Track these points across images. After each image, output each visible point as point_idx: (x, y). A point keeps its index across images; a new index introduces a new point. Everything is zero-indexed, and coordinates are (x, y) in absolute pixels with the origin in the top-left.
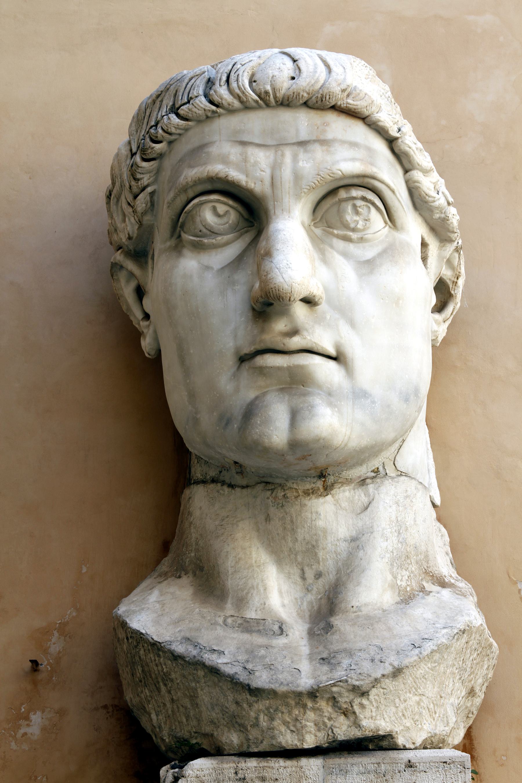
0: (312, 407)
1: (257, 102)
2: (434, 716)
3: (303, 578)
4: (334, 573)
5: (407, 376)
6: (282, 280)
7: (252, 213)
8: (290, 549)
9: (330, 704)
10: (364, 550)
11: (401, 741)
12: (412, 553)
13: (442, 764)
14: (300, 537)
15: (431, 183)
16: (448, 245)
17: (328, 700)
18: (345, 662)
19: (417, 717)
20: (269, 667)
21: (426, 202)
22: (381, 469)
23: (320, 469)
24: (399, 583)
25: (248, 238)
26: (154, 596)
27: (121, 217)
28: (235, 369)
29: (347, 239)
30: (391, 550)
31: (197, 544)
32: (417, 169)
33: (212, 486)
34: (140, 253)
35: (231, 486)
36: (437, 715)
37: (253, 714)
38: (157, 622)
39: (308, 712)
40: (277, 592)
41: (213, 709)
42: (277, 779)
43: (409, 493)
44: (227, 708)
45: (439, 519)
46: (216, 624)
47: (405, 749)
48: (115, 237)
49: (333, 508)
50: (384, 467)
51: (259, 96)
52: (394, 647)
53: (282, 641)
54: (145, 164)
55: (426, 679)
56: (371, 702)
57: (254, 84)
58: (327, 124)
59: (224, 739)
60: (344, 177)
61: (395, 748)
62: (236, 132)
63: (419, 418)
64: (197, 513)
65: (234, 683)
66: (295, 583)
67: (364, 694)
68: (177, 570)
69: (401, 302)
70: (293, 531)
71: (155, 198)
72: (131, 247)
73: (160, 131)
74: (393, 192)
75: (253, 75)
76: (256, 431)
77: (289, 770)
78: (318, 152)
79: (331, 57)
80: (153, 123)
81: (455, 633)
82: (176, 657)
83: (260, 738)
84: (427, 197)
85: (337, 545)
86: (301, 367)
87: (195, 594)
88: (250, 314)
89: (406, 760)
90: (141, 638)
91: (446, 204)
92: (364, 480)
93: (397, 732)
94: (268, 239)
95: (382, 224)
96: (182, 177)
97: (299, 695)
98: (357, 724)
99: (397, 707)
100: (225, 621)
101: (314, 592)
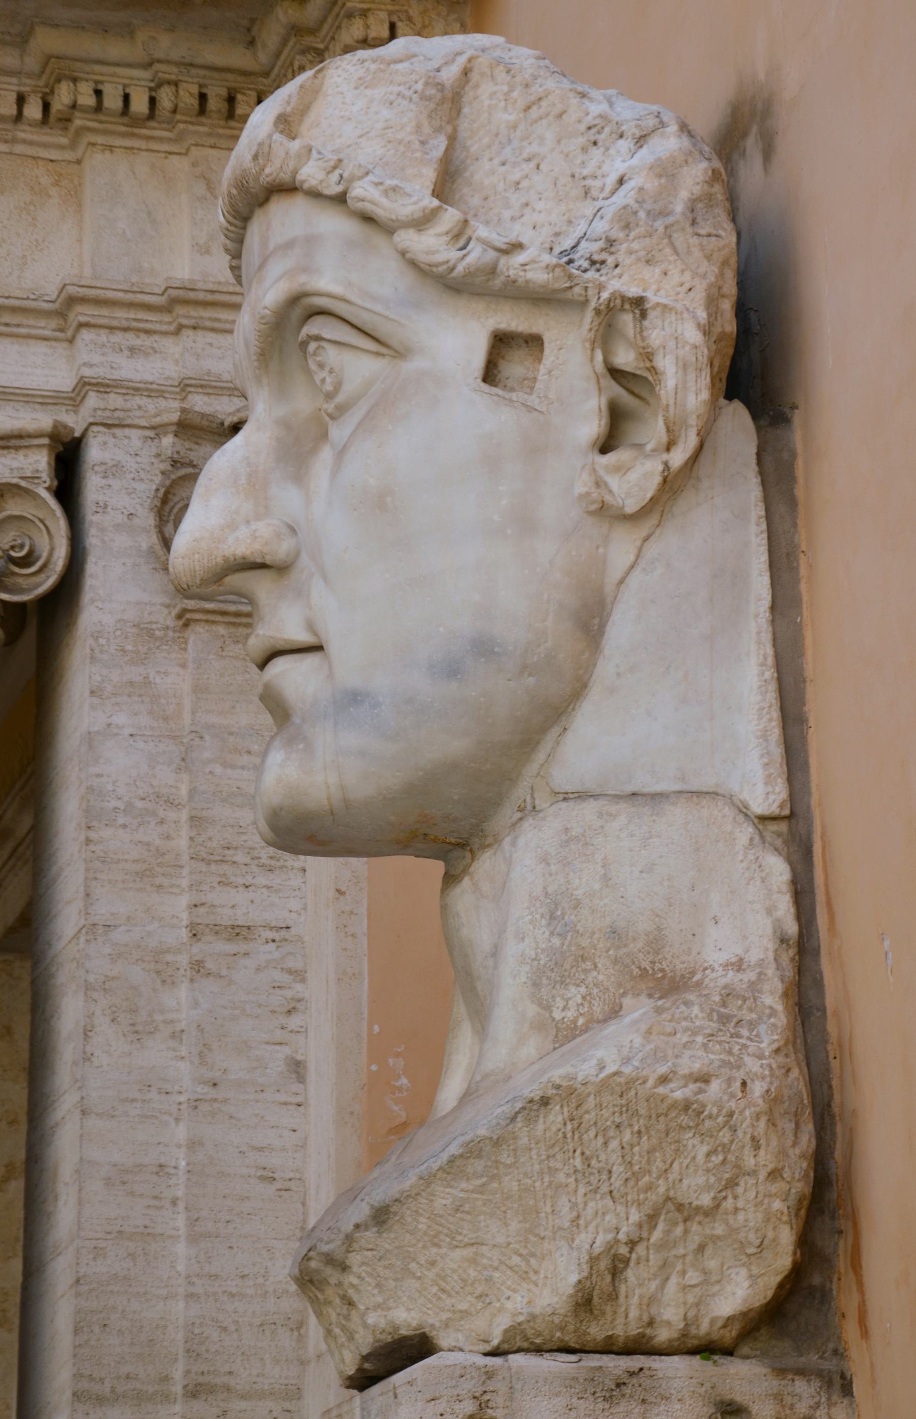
2: (534, 1278)
5: (441, 629)
12: (601, 945)
19: (479, 1289)
24: (557, 1015)
30: (533, 956)
32: (399, 228)
36: (542, 1276)
55: (467, 1213)
69: (389, 499)
81: (517, 1109)
84: (434, 269)
91: (491, 254)
93: (432, 1325)
99: (419, 1278)
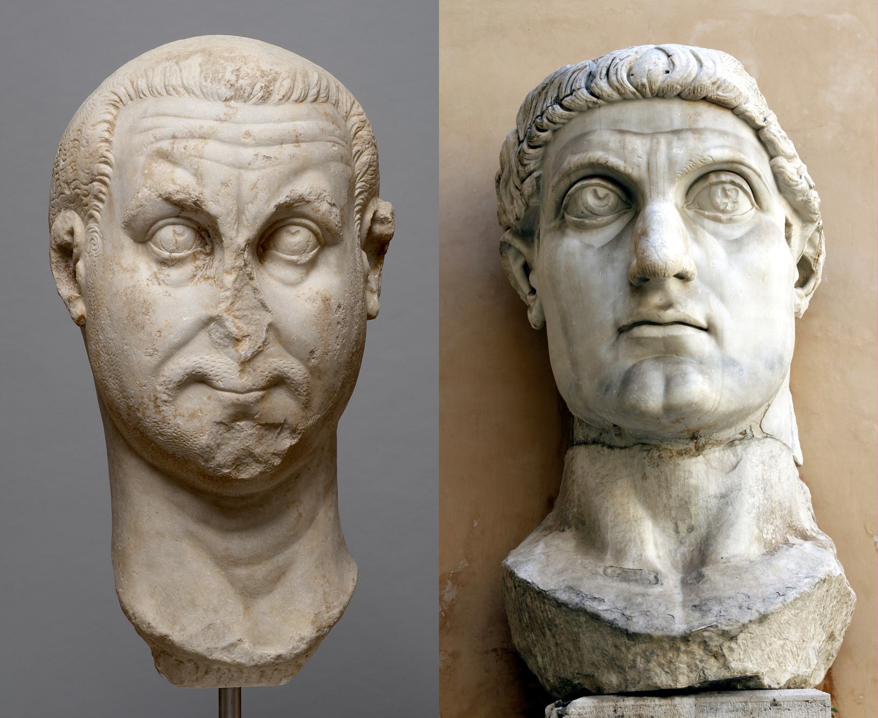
0: (685, 374)
1: (634, 94)
3: (677, 531)
4: (705, 527)
6: (657, 258)
7: (630, 196)
11: (766, 681)
14: (674, 494)
15: (795, 169)
16: (810, 225)
17: (700, 644)
18: (716, 609)
19: (781, 660)
20: (646, 613)
21: (790, 186)
22: (748, 431)
23: (691, 432)
25: (626, 219)
26: (540, 548)
27: (509, 200)
28: (614, 339)
29: (717, 220)
31: (579, 500)
33: (593, 447)
34: (527, 233)
35: (611, 447)
37: (630, 657)
38: (542, 572)
39: (681, 655)
40: (653, 545)
41: (594, 651)
43: (774, 453)
45: (802, 477)
46: (596, 573)
47: (770, 688)
48: (504, 218)
49: (704, 466)
51: (636, 89)
52: (760, 595)
53: (657, 589)
54: (531, 151)
56: (739, 646)
57: (632, 77)
58: (698, 114)
59: (604, 680)
60: (715, 163)
61: (761, 688)
62: (616, 122)
63: (784, 384)
64: (579, 472)
66: (670, 536)
67: (733, 638)
68: (560, 524)
70: (668, 488)
71: (541, 182)
72: (519, 228)
73: (545, 120)
74: (760, 176)
75: (630, 69)
76: (633, 397)
77: (664, 708)
78: (691, 140)
79: (702, 52)
80: (539, 113)
82: (560, 605)
83: (638, 679)
86: (675, 338)
87: (577, 546)
88: (628, 289)
89: (771, 699)
92: (733, 442)
94: (644, 220)
95: (750, 206)
96: (566, 163)
97: (673, 639)
100: (605, 571)
101: (687, 545)
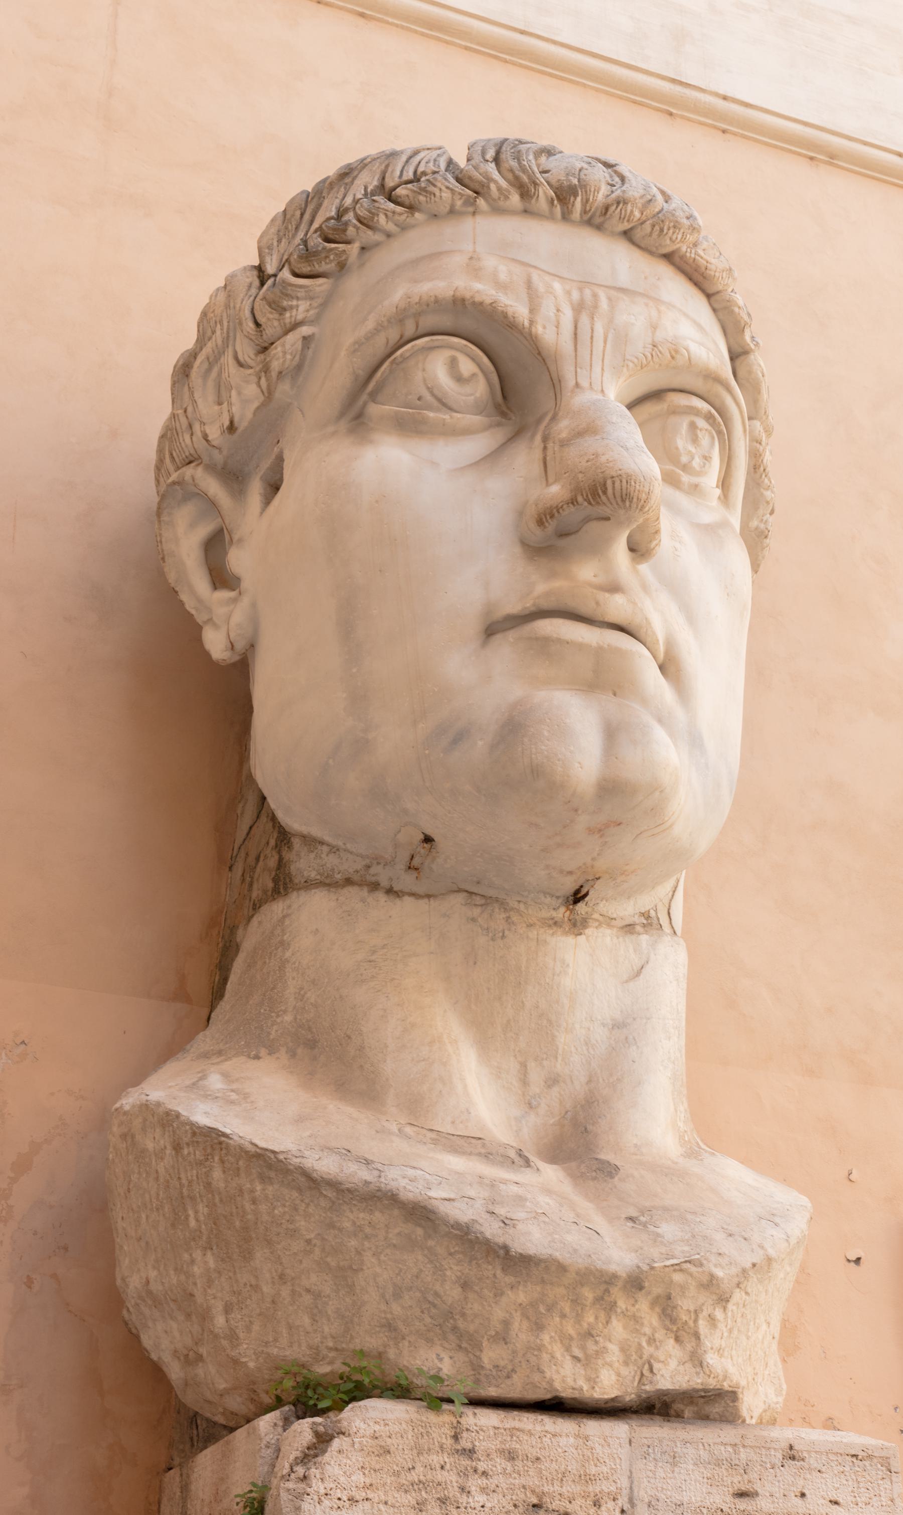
3: (524, 1082)
8: (509, 1021)
9: (658, 1309)
10: (638, 1047)
13: (849, 1458)
22: (652, 913)
42: (538, 1459)
44: (436, 1294)
50: (656, 911)
56: (726, 1318)
65: (466, 1239)
77: (563, 1441)
85: (589, 1029)
88: (518, 550)
89: (785, 1445)
90: (221, 1143)
98: (696, 1360)
